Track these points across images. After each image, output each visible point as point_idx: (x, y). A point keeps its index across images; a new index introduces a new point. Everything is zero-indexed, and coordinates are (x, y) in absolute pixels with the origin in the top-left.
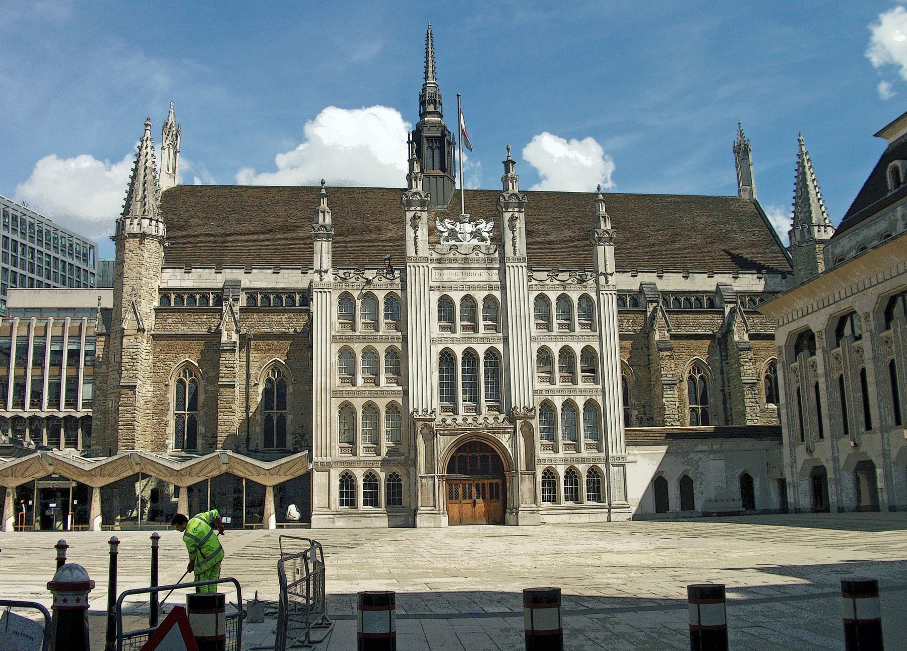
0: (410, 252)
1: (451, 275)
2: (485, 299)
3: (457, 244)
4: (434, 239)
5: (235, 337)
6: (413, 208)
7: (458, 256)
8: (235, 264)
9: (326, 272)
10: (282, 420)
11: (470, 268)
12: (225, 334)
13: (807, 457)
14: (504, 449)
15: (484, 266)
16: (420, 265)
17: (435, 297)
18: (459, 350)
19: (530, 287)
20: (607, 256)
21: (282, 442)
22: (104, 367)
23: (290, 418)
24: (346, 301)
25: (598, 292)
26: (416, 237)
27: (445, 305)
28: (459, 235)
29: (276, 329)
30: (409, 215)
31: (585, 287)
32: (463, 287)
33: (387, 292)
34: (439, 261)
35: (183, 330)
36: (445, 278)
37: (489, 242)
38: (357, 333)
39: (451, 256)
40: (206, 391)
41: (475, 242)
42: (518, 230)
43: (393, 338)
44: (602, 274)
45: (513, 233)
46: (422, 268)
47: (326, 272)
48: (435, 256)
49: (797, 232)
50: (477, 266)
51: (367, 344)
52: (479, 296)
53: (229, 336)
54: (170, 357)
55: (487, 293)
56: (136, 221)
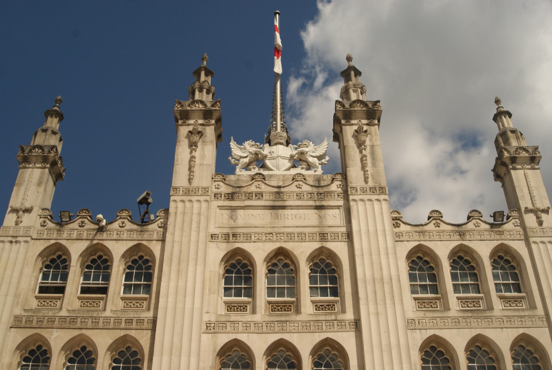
0: (180, 178)
2: (312, 258)
3: (265, 173)
4: (224, 166)
6: (192, 122)
7: (264, 188)
9: (28, 211)
11: (284, 207)
15: (311, 203)
16: (194, 198)
17: (217, 252)
19: (398, 235)
20: (532, 184)
24: (55, 262)
25: (527, 240)
26: (192, 158)
27: (238, 271)
28: (268, 162)
30: (183, 131)
31: (501, 233)
32: (270, 236)
33: (131, 244)
34: (231, 196)
36: (240, 221)
37: (320, 171)
38: (64, 313)
39: (253, 189)
42: (368, 149)
43: (129, 321)
44: (527, 211)
45: (361, 152)
46: (196, 205)
47: (28, 211)
48: (224, 189)
50: (299, 203)
51: (77, 333)
52: (302, 251)
55: (316, 245)
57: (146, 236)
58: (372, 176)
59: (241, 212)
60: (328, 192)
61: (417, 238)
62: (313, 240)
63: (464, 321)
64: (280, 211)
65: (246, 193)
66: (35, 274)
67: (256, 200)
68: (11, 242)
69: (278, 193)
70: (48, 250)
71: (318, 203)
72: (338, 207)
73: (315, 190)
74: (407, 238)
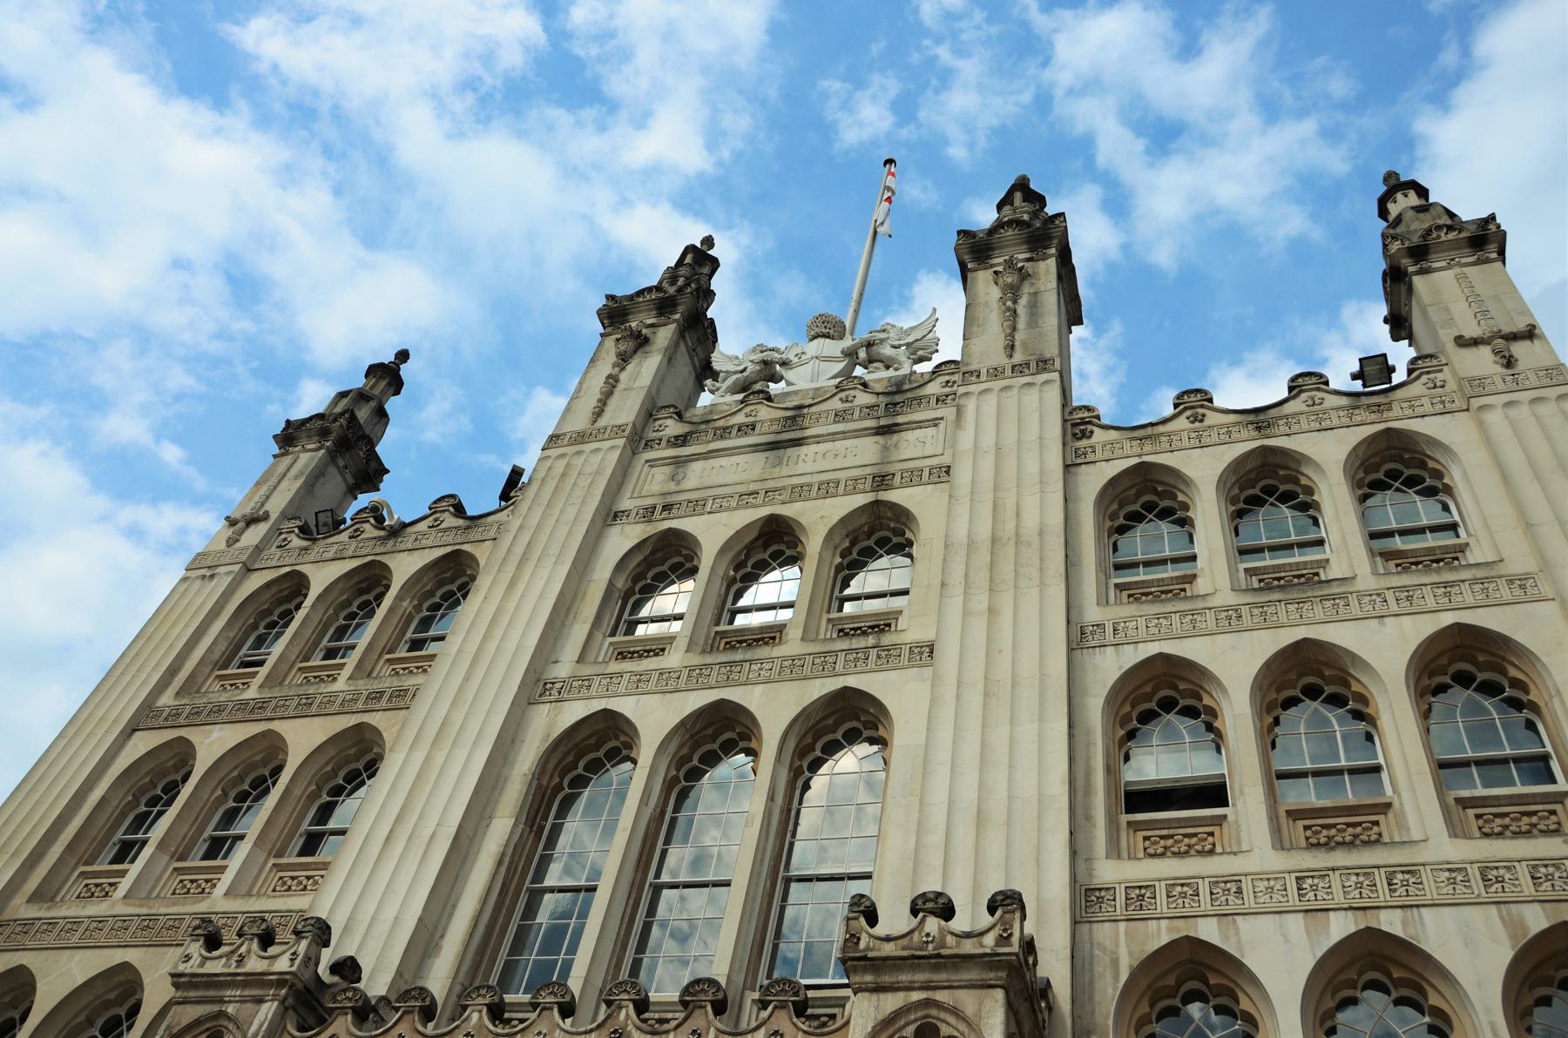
50: (840, 427)
57: (475, 534)
58: (1024, 344)
59: (697, 466)
60: (914, 399)
61: (1136, 450)
62: (855, 491)
63: (1256, 611)
64: (790, 451)
65: (716, 429)
66: (232, 635)
67: (737, 436)
68: (204, 577)
69: (793, 418)
70: (274, 590)
71: (883, 422)
72: (935, 422)
73: (883, 400)
74: (1107, 455)
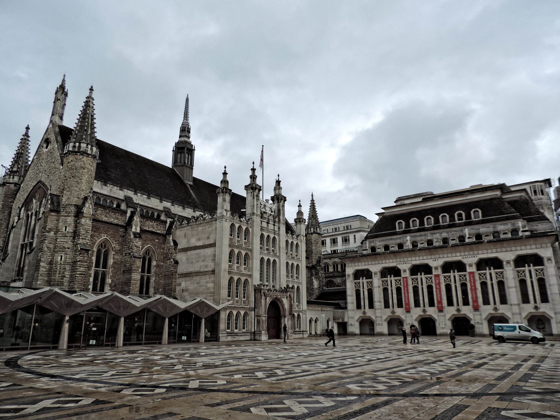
1: (264, 224)
5: (138, 231)
8: (129, 187)
10: (148, 279)
12: (134, 227)
13: (362, 315)
14: (283, 305)
18: (266, 258)
21: (147, 292)
22: (52, 233)
23: (153, 280)
29: (151, 229)
35: (105, 219)
36: (263, 225)
40: (114, 258)
41: (270, 213)
49: (312, 229)
53: (136, 229)
54: (96, 234)
56: (89, 146)
